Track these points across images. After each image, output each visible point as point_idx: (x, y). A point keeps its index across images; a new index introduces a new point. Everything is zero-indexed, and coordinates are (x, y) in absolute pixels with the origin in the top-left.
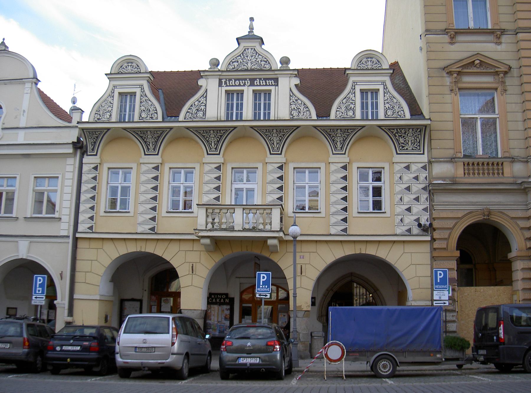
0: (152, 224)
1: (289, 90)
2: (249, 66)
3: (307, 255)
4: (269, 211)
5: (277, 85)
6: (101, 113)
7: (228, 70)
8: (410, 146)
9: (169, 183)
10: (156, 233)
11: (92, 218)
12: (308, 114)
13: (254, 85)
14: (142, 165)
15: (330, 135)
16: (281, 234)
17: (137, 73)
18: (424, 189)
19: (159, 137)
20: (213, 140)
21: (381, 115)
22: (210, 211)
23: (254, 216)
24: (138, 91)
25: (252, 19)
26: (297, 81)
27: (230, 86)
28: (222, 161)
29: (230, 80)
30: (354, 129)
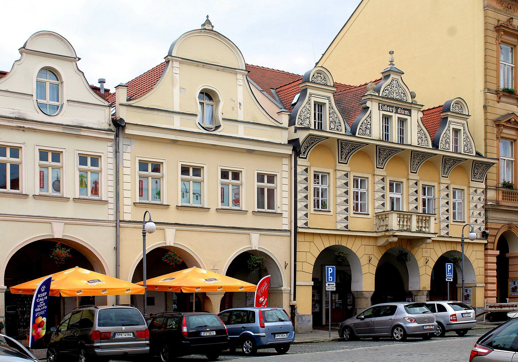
2: (395, 96)
8: (478, 176)
10: (350, 231)
18: (483, 207)
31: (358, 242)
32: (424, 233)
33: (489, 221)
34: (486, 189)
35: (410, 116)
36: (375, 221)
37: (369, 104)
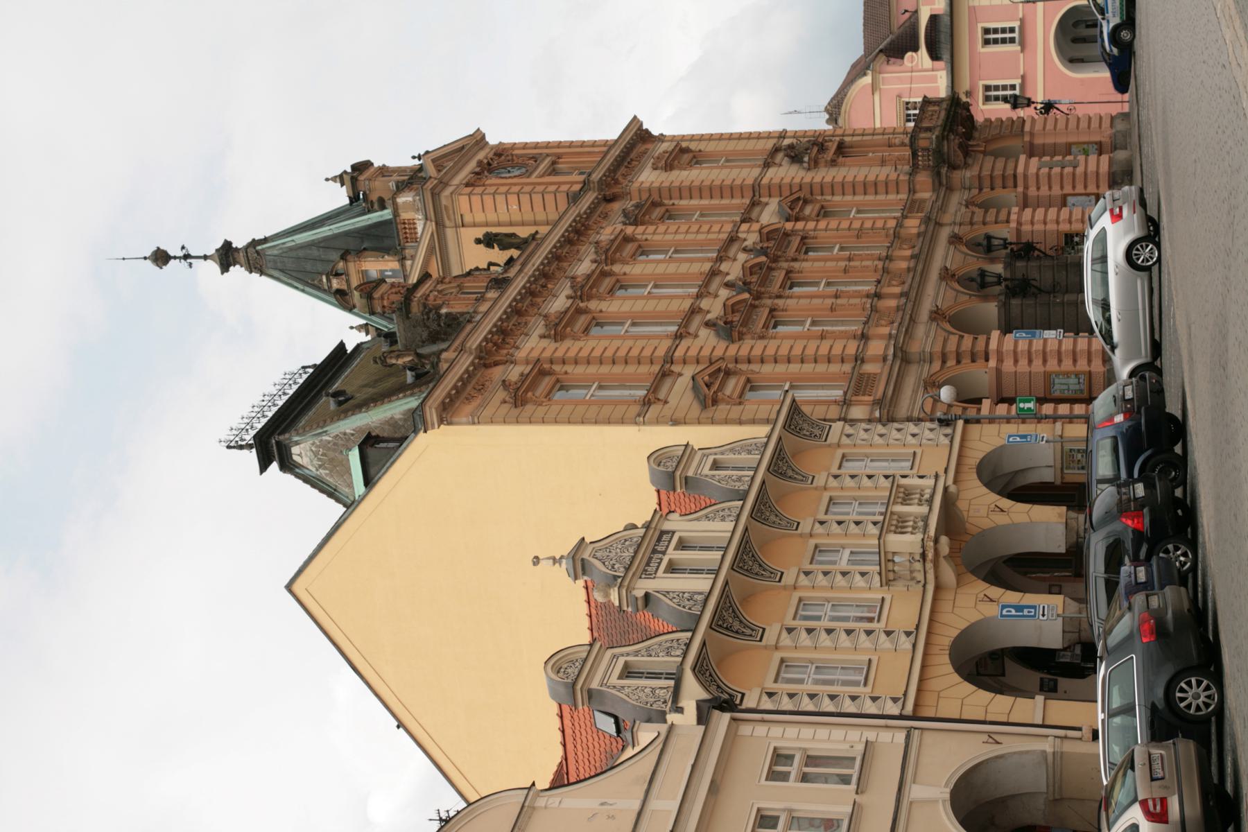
31: (945, 616)
32: (932, 496)
33: (915, 414)
34: (845, 420)
35: (674, 532)
36: (899, 587)
37: (639, 593)
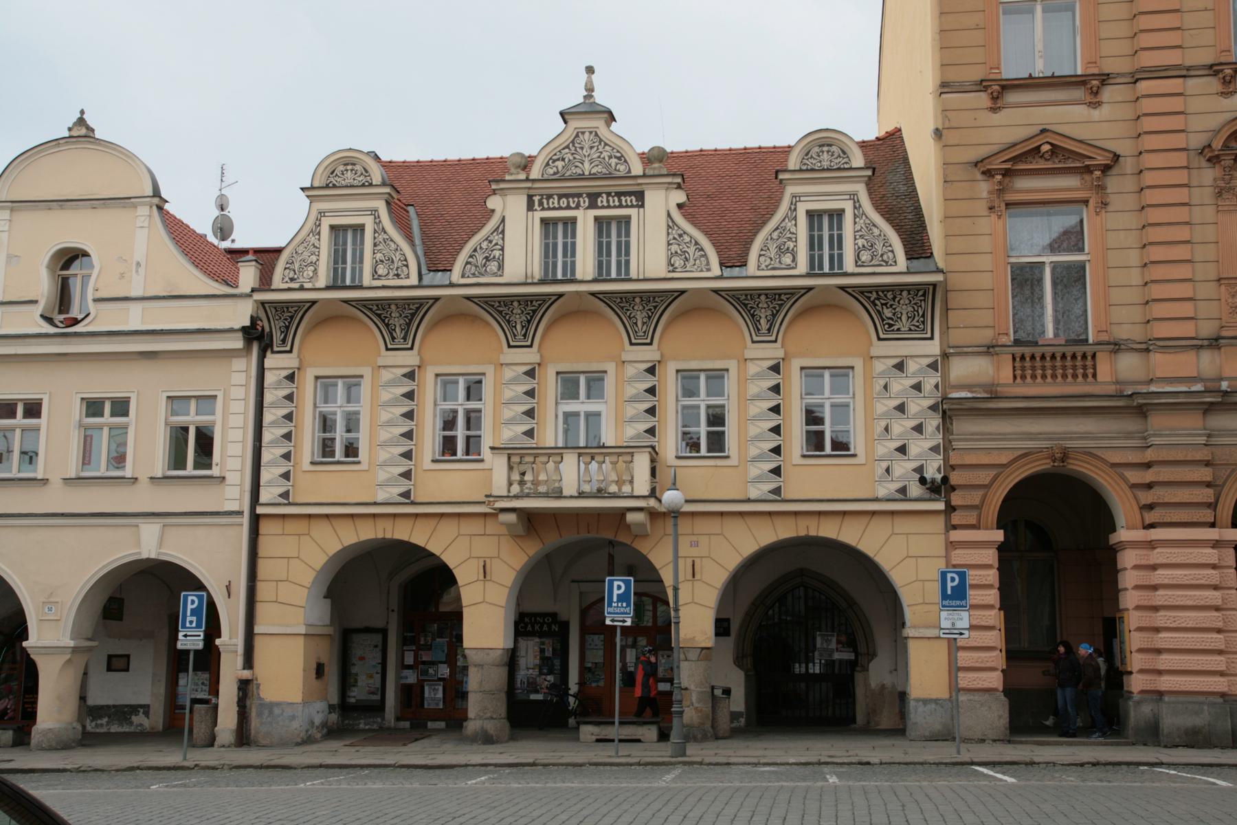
0: (404, 486)
1: (664, 215)
3: (704, 540)
4: (628, 458)
5: (642, 206)
6: (297, 266)
7: (546, 176)
8: (904, 324)
9: (435, 405)
10: (413, 503)
11: (286, 476)
12: (704, 263)
13: (596, 207)
14: (383, 371)
15: (746, 305)
16: (652, 503)
17: (363, 185)
18: (933, 408)
19: (413, 315)
20: (519, 320)
21: (849, 266)
22: (515, 459)
23: (600, 468)
24: (368, 222)
25: (590, 70)
26: (680, 197)
27: (549, 209)
28: (537, 359)
29: (549, 197)
30: (792, 294)
31: (448, 530)
33: (956, 445)
